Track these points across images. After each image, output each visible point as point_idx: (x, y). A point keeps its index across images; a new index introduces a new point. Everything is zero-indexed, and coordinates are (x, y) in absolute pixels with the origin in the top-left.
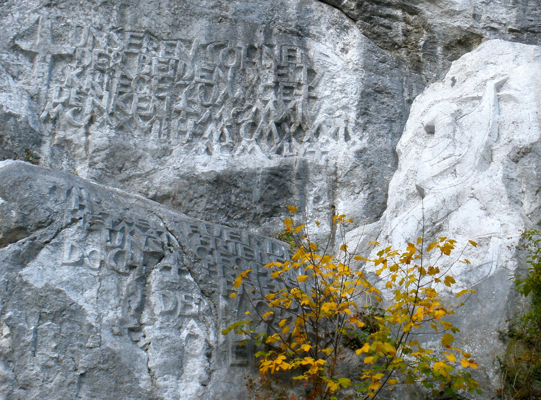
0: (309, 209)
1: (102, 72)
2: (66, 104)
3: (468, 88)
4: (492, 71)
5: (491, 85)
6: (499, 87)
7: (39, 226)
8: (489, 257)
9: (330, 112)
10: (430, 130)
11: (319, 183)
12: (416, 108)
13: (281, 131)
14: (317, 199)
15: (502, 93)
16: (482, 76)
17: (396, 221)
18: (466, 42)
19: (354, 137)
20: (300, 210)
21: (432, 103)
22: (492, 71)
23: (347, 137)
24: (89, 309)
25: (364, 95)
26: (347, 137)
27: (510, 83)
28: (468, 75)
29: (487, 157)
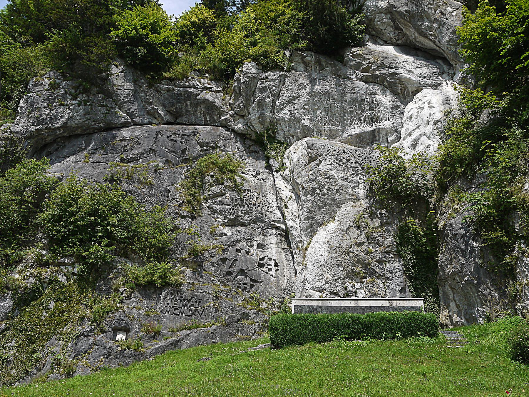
0: (381, 140)
1: (326, 111)
2: (318, 121)
3: (420, 104)
4: (426, 99)
5: (426, 103)
6: (429, 103)
7: (320, 156)
8: (430, 151)
9: (384, 114)
10: (411, 117)
11: (383, 133)
12: (406, 111)
13: (372, 121)
14: (383, 137)
15: (430, 105)
16: (424, 101)
17: (404, 142)
18: (418, 91)
19: (391, 120)
20: (379, 140)
21: (411, 108)
22: (426, 99)
23: (389, 120)
24: (335, 175)
25: (392, 109)
26: (389, 120)
27: (431, 102)
28: (420, 100)
29: (428, 122)
